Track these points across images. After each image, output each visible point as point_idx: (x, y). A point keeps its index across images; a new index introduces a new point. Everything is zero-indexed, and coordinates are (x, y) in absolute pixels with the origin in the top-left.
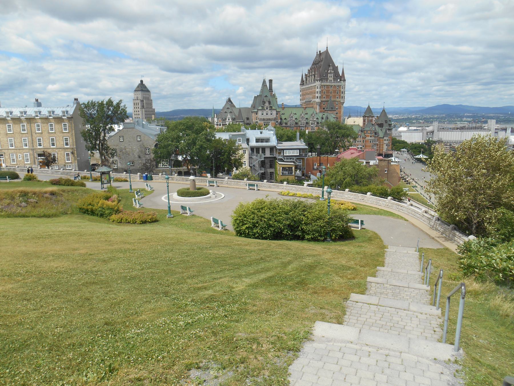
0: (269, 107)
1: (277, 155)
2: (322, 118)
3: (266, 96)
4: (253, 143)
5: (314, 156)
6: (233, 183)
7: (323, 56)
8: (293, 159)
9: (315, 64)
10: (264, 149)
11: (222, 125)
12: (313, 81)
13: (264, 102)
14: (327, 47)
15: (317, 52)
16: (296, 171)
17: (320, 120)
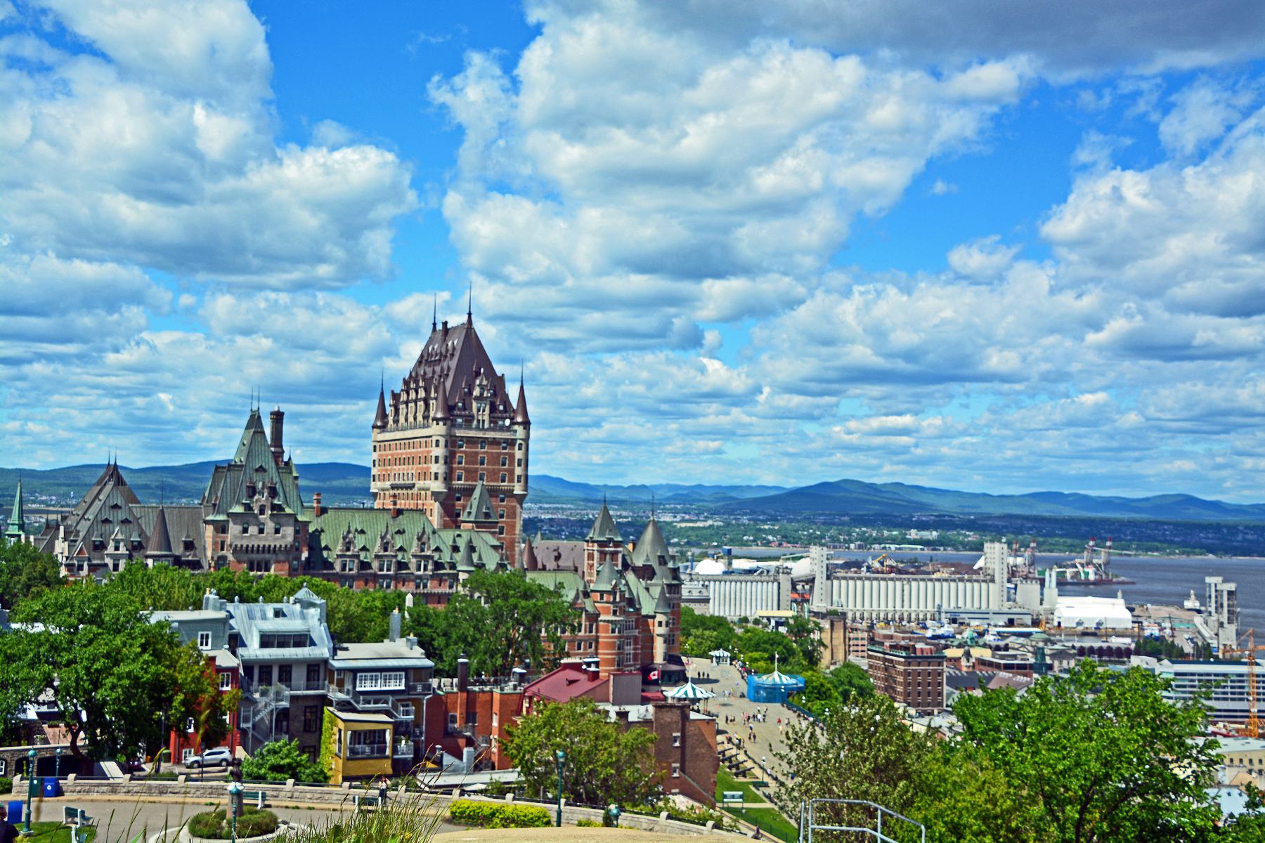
0: (268, 505)
1: (333, 687)
2: (455, 549)
3: (261, 469)
4: (253, 650)
5: (448, 689)
6: (309, 795)
7: (455, 341)
8: (386, 702)
9: (428, 363)
10: (286, 669)
11: (90, 566)
12: (420, 418)
13: (252, 491)
14: (470, 314)
15: (435, 324)
16: (396, 741)
17: (446, 557)
